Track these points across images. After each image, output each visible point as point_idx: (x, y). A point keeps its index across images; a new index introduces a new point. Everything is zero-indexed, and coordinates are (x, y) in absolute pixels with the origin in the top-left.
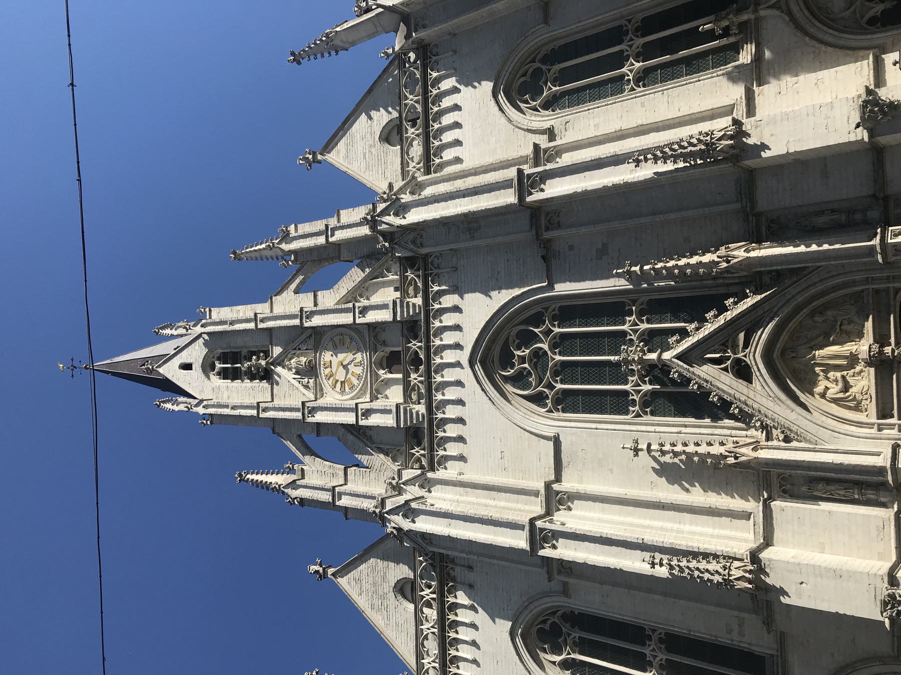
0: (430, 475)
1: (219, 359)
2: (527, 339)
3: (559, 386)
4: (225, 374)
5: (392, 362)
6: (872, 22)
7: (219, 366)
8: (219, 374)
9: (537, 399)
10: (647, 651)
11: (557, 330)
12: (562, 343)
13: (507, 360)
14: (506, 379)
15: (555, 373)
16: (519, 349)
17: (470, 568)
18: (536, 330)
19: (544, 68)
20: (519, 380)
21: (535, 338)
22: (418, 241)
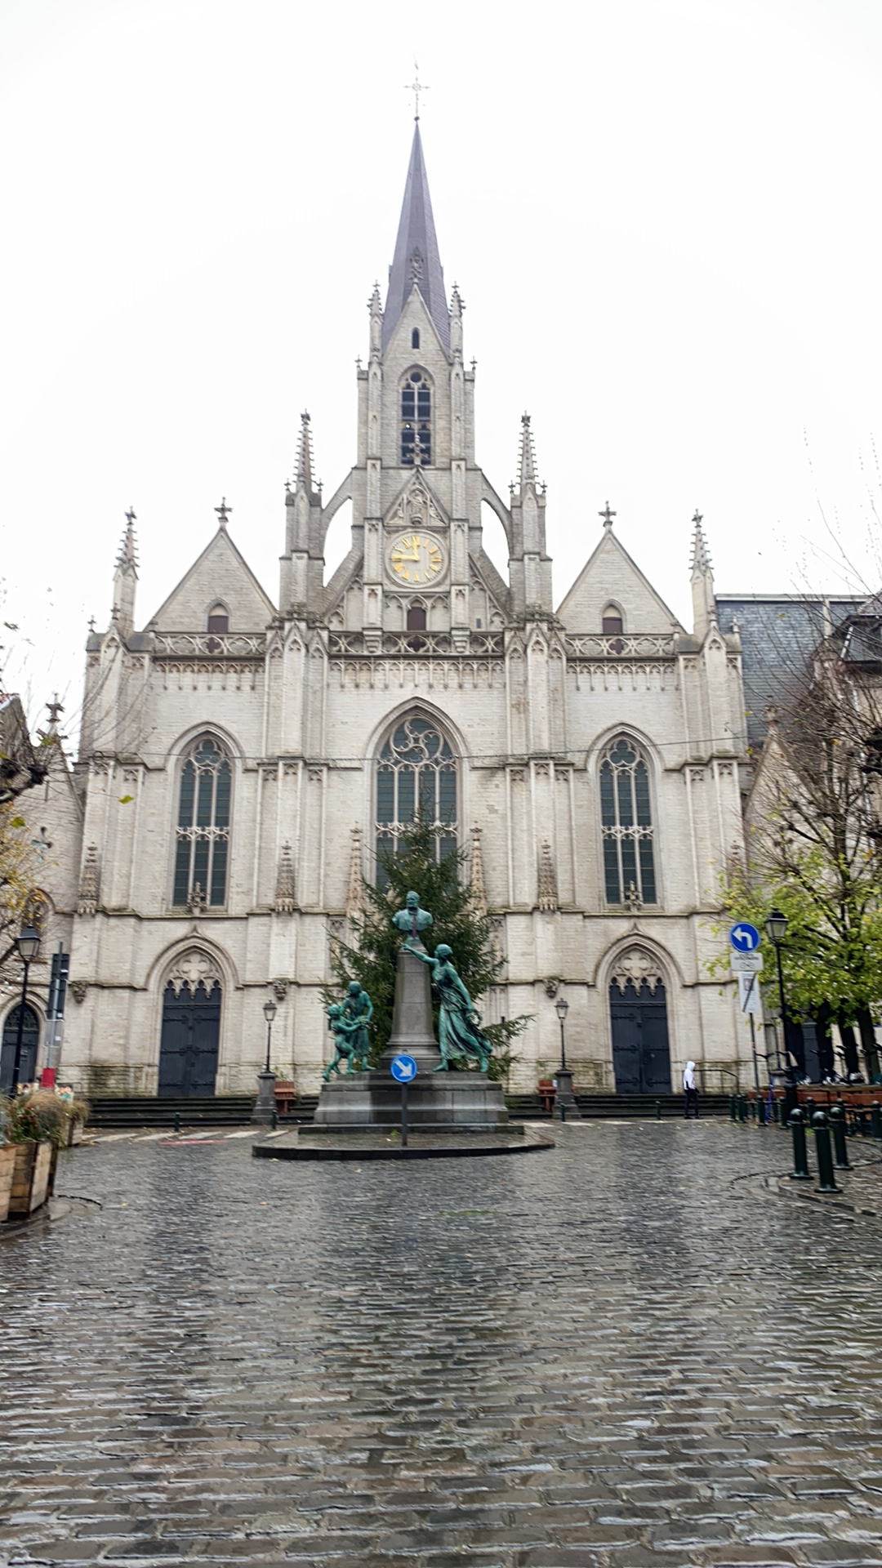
0: (326, 658)
1: (424, 387)
2: (432, 743)
3: (396, 769)
4: (407, 396)
5: (417, 616)
6: (614, 980)
7: (416, 386)
8: (408, 387)
9: (386, 752)
10: (213, 828)
11: (437, 769)
12: (427, 774)
13: (418, 725)
14: (402, 725)
15: (406, 767)
16: (427, 737)
17: (253, 688)
18: (438, 754)
19: (634, 765)
20: (401, 738)
21: (432, 753)
22: (515, 655)
